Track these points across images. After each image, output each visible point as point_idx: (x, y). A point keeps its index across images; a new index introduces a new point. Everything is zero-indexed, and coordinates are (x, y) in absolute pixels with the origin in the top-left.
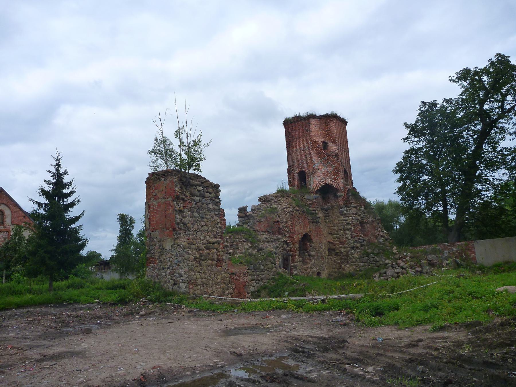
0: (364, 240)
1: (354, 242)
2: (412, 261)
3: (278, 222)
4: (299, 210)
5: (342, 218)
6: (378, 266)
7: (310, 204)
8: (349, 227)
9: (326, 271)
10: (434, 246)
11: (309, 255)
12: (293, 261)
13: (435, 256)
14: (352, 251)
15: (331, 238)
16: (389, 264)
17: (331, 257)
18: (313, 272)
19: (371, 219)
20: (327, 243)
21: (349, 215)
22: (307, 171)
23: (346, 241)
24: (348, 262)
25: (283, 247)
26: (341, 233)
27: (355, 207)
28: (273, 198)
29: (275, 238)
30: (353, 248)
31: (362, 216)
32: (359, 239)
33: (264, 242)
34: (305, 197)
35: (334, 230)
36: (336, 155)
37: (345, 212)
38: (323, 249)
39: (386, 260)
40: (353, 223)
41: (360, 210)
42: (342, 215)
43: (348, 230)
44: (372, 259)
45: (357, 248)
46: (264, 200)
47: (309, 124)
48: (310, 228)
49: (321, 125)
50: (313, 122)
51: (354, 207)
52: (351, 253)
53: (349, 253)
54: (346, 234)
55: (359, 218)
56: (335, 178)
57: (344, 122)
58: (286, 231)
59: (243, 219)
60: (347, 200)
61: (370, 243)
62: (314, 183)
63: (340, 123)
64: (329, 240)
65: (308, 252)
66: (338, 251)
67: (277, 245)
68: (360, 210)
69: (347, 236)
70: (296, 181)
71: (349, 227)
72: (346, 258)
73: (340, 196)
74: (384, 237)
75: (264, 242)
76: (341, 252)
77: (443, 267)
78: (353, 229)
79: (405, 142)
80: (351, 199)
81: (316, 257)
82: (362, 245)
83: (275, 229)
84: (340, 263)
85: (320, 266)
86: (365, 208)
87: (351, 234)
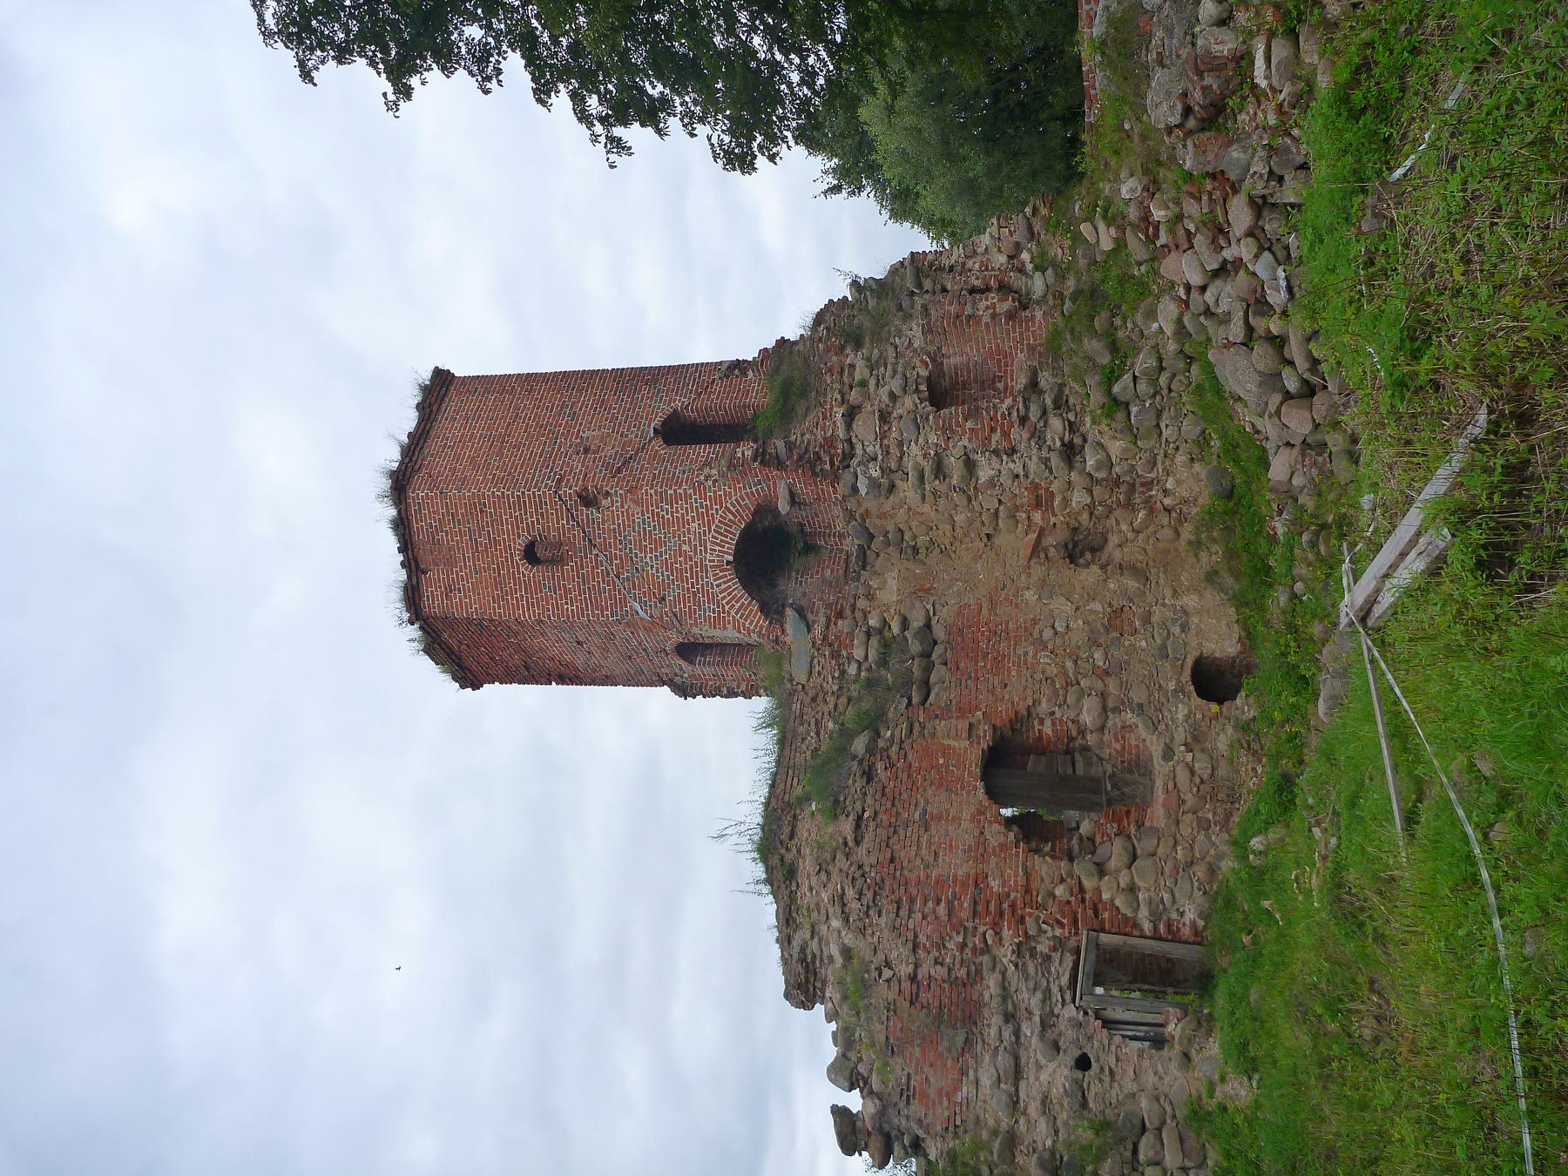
0: (1033, 384)
1: (1041, 441)
2: (1178, 202)
3: (913, 978)
4: (860, 818)
5: (907, 490)
6: (1190, 360)
7: (836, 655)
8: (954, 464)
9: (1191, 601)
10: (1085, 51)
11: (1102, 728)
12: (1128, 926)
13: (1159, 75)
14: (1090, 462)
15: (1015, 541)
16: (1179, 321)
17: (1114, 540)
18: (1196, 740)
19: (915, 331)
20: (1038, 571)
21: (894, 450)
22: (675, 638)
23: (1035, 487)
24: (1149, 485)
25: (1048, 958)
26: (988, 501)
27: (851, 415)
28: (796, 951)
29: (997, 1020)
30: (1070, 452)
31: (895, 385)
32: (1023, 420)
33: (1014, 1103)
34: (801, 677)
35: (971, 522)
36: (588, 501)
37: (875, 473)
38: (1067, 605)
39: (1152, 315)
40: (933, 439)
41: (863, 384)
42: (892, 487)
43: (970, 465)
44: (1142, 387)
45: (1072, 427)
46: (803, 990)
47: (450, 622)
48: (957, 737)
49: (451, 563)
50: (434, 602)
51: (849, 426)
52: (1098, 468)
53: (1100, 475)
54: (992, 483)
55: (909, 402)
56: (700, 516)
57: (440, 386)
58: (964, 945)
59: (897, 1148)
60: (809, 463)
61: (1052, 351)
62: (731, 613)
63: (433, 445)
64: (1025, 552)
65: (1082, 732)
66: (1085, 516)
67: (1035, 1002)
68: (863, 384)
69: (1005, 479)
70: (732, 673)
71: (954, 464)
72: (1129, 490)
73: (792, 495)
74: (1018, 247)
75: (1014, 1103)
76: (1091, 508)
77: (1243, 59)
78: (965, 442)
79: (499, 72)
80: (807, 432)
81: (1112, 686)
82: (1060, 404)
83: (953, 1013)
84: (1151, 511)
85: (1163, 652)
86: (858, 345)
87: (996, 452)
